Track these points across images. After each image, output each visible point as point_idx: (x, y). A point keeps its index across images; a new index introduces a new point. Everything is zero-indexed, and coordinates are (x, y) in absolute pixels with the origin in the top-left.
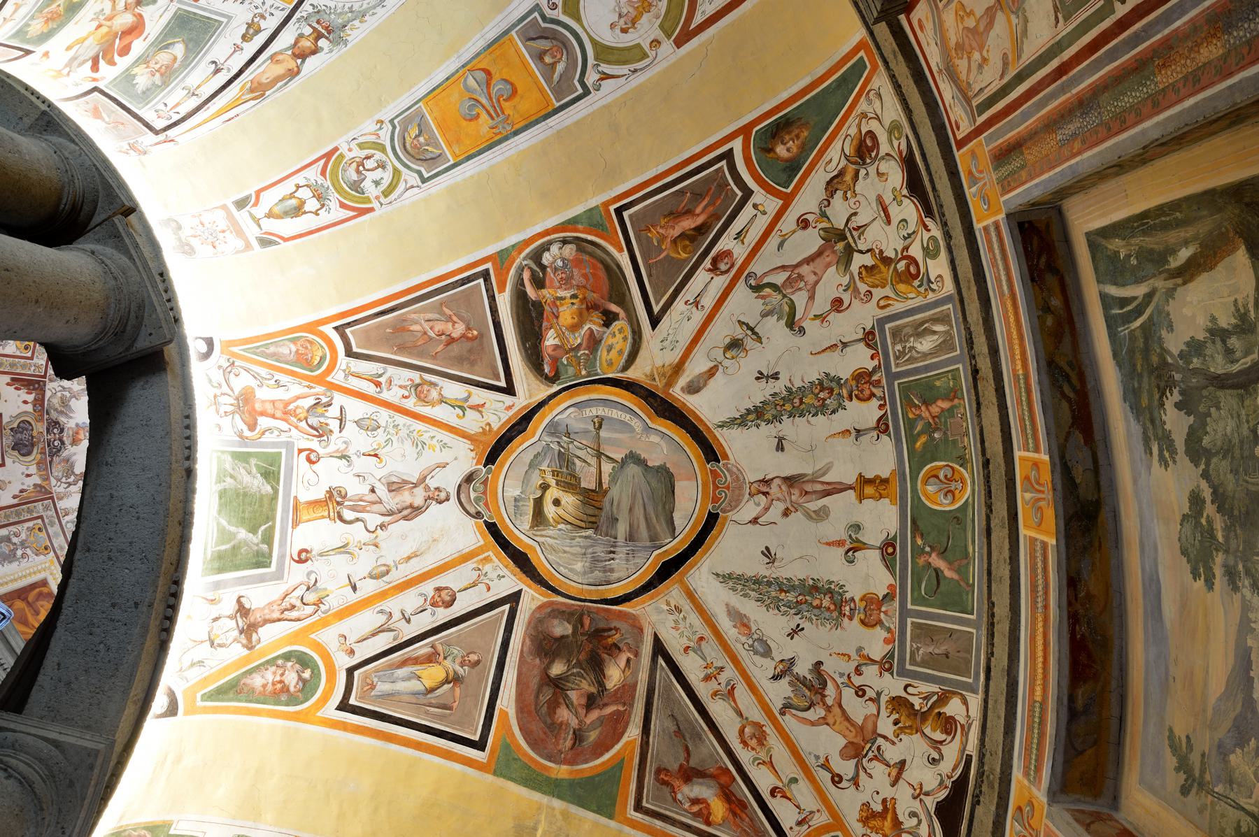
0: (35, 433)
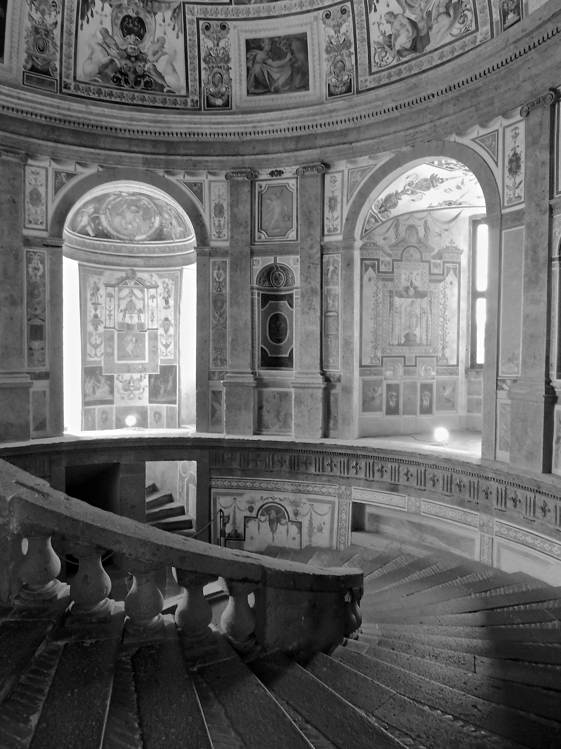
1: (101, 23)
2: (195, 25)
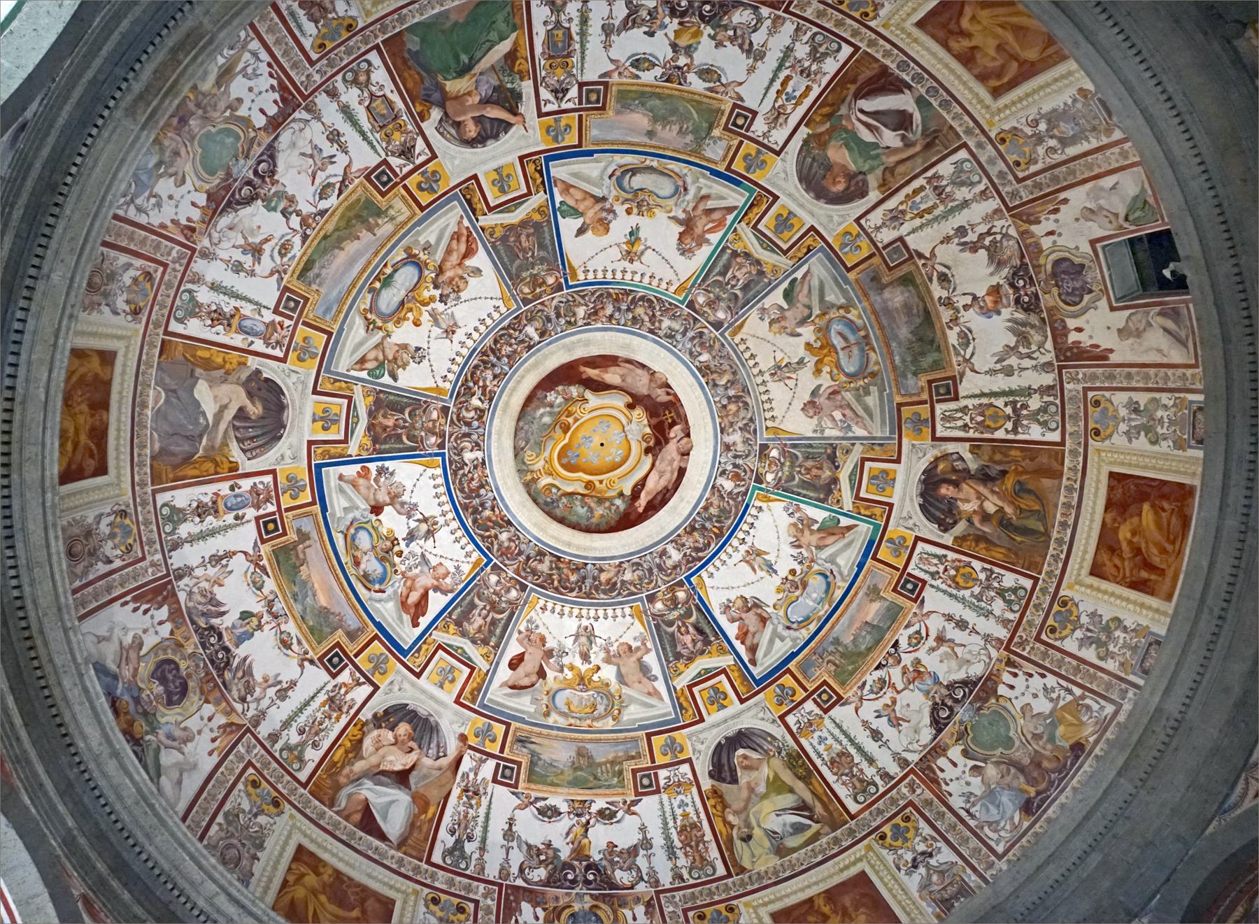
0: (1055, 291)
1: (145, 631)
2: (241, 766)
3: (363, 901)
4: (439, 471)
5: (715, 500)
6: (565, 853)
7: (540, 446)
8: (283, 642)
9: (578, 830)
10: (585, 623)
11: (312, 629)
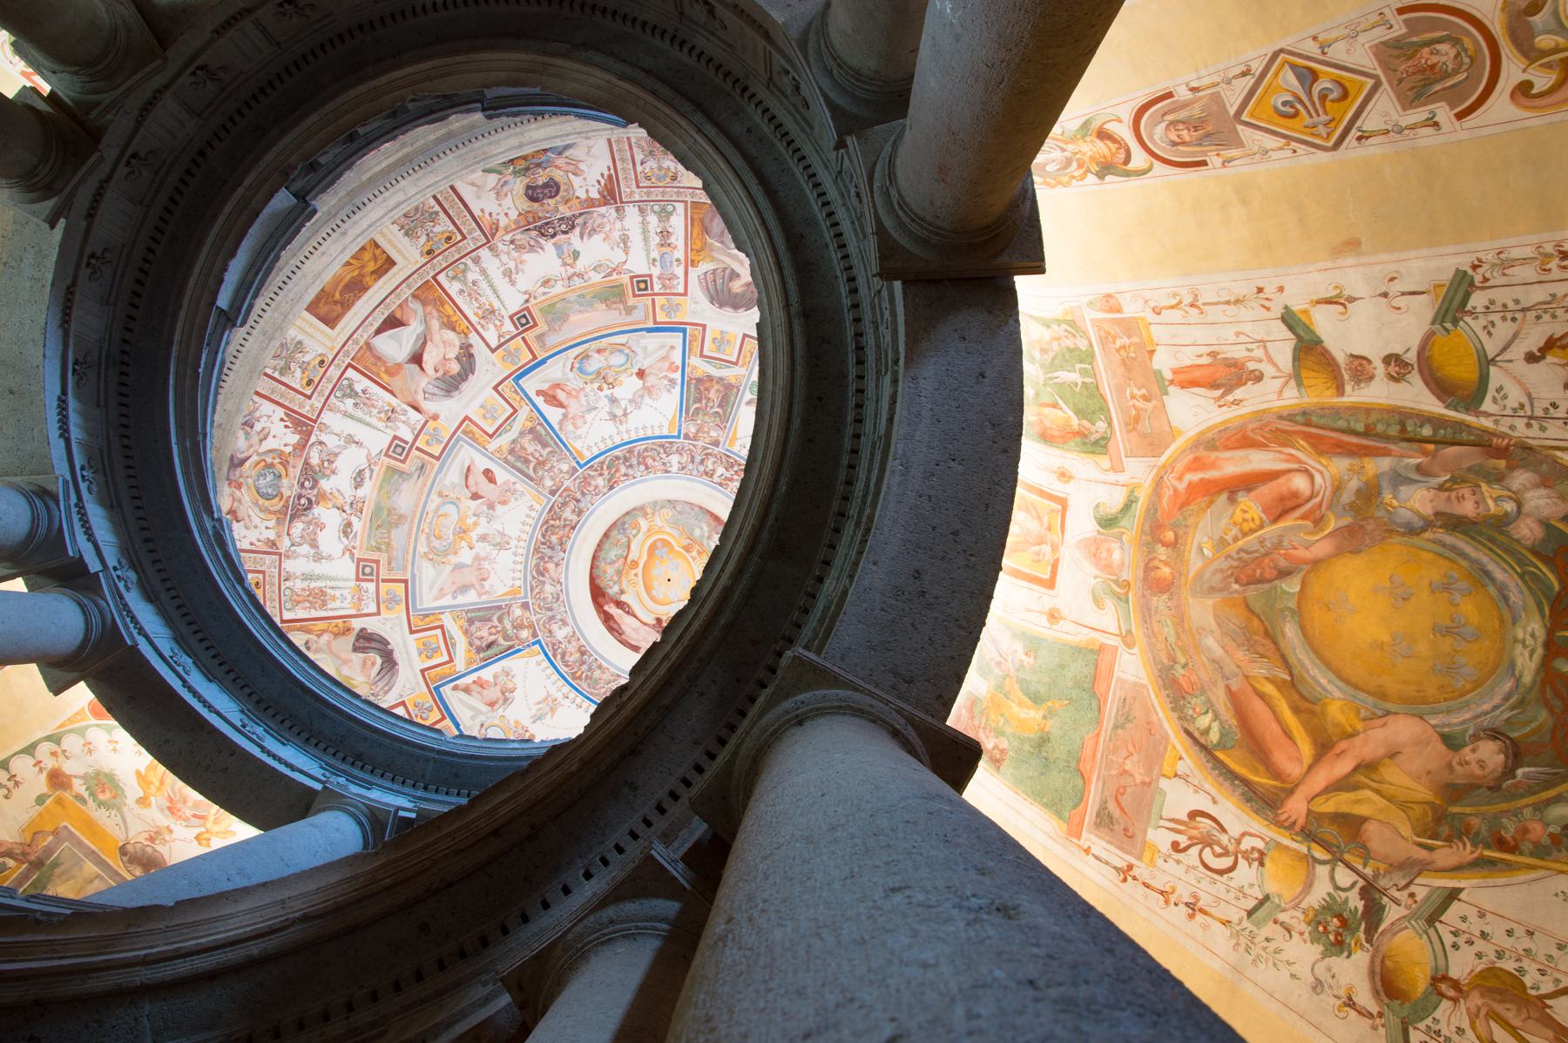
3: (342, 304)
4: (665, 432)
5: (606, 676)
6: (325, 484)
7: (675, 524)
8: (548, 281)
9: (340, 502)
10: (513, 543)
11: (553, 305)
